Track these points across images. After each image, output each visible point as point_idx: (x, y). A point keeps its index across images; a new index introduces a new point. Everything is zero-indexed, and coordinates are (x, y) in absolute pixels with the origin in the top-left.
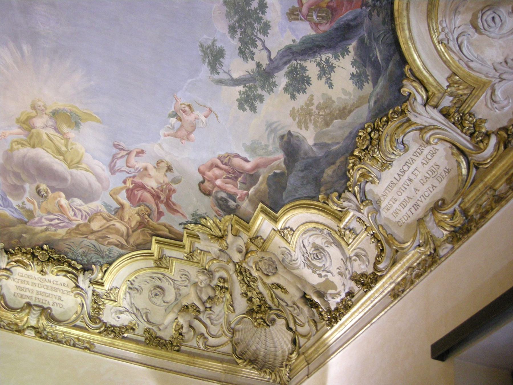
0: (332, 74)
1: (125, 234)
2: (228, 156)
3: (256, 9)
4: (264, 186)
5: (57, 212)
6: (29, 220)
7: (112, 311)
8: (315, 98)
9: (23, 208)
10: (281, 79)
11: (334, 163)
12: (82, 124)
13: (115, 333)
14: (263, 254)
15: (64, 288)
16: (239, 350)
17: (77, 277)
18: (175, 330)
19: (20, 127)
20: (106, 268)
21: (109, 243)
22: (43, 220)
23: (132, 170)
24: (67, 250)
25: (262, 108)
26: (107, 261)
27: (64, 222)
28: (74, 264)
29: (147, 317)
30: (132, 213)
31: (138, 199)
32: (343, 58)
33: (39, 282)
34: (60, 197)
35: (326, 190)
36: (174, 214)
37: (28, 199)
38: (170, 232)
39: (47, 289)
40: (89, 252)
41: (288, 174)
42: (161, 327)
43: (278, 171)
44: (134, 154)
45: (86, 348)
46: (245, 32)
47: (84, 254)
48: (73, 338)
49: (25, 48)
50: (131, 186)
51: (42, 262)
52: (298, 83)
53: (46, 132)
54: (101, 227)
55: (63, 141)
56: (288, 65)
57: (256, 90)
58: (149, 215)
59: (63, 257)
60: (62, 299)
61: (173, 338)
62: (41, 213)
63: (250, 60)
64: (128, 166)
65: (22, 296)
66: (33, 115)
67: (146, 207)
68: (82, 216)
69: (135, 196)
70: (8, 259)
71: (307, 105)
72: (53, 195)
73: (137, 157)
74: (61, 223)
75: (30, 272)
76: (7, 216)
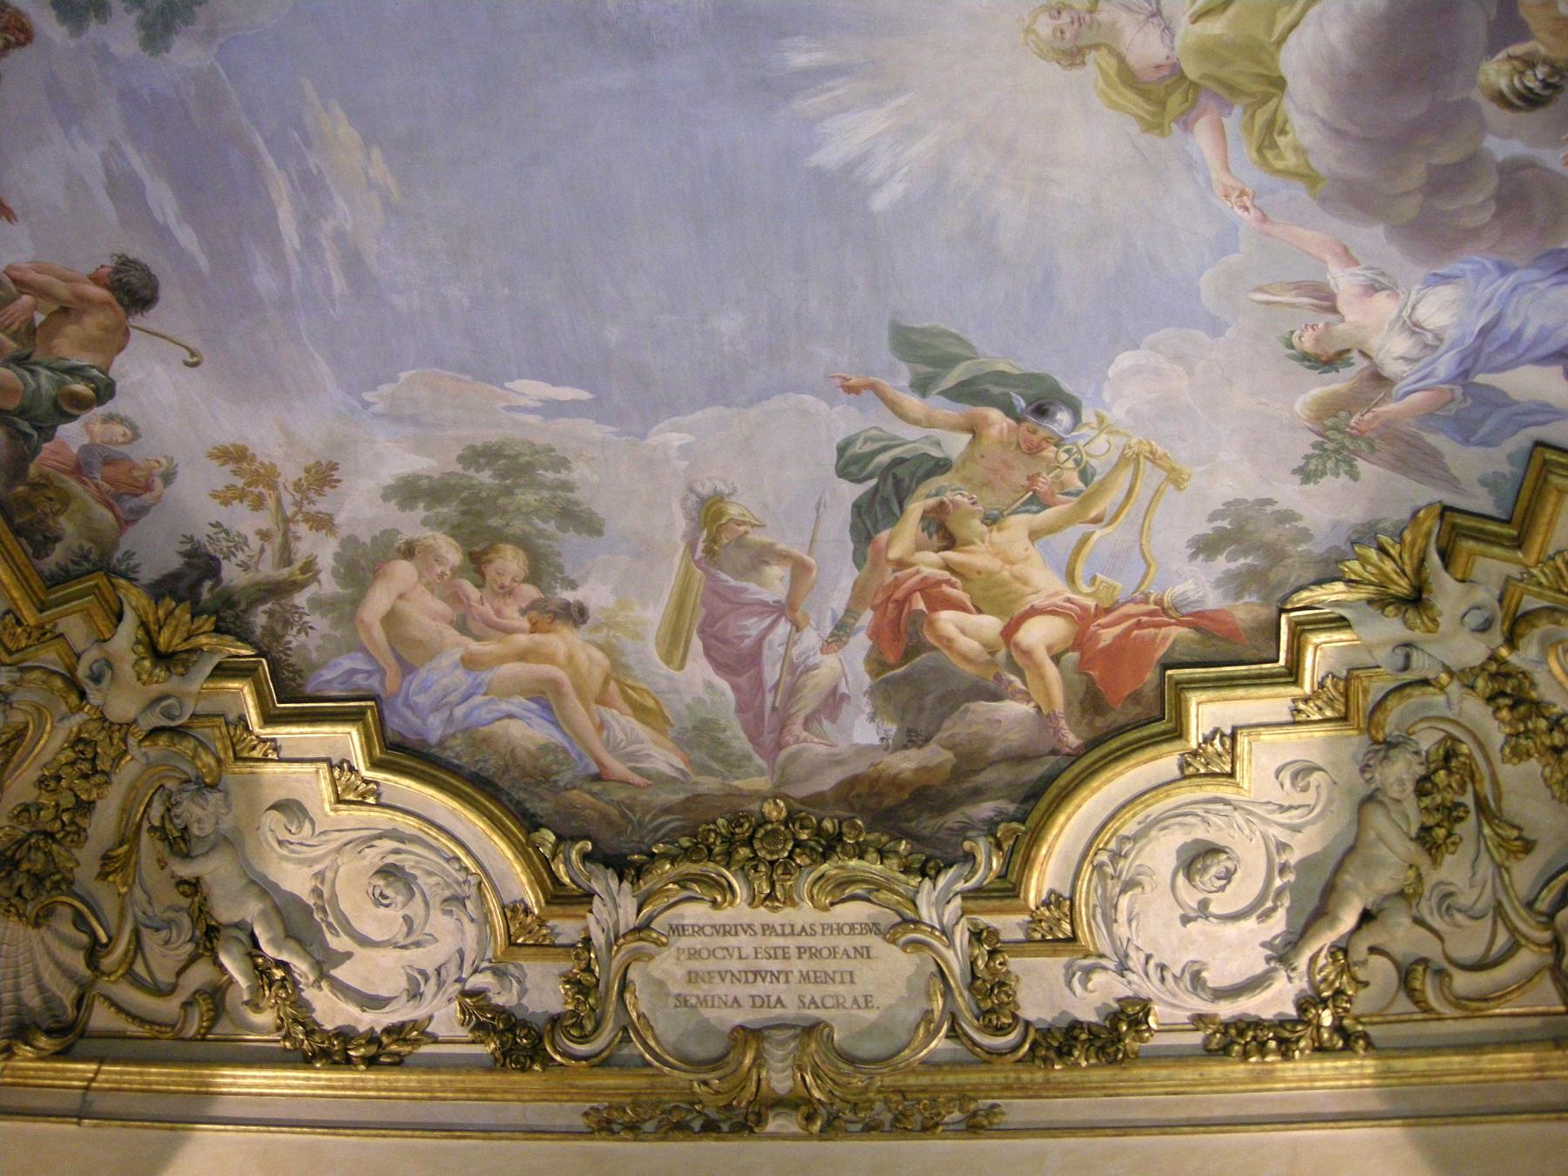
19: (1187, 127)
53: (1185, 19)
66: (1114, 62)
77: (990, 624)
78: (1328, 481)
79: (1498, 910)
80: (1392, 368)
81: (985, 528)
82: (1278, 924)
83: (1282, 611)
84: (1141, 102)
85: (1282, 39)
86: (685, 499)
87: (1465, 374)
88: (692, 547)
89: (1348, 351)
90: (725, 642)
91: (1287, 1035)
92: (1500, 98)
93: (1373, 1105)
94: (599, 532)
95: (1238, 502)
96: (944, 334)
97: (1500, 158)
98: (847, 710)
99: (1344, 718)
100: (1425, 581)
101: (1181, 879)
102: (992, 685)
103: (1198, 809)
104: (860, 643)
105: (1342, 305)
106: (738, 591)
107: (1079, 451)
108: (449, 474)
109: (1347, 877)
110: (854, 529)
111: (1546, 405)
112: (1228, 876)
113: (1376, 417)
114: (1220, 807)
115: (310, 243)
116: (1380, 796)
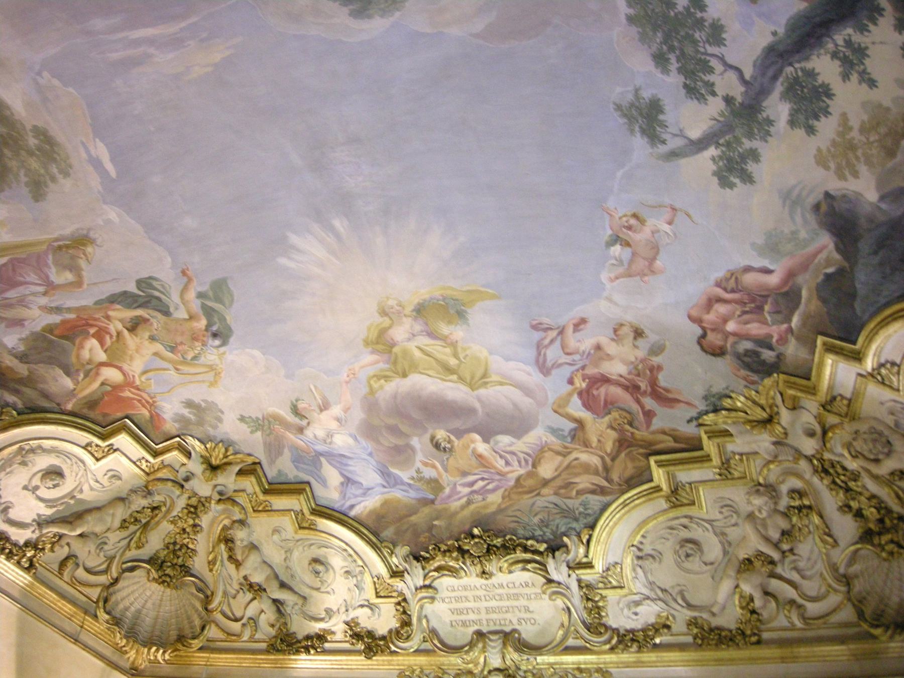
0: (867, 61)
1: (600, 468)
2: (732, 274)
3: (687, 9)
5: (477, 468)
6: (436, 495)
7: (621, 605)
8: (850, 116)
9: (421, 479)
10: (778, 108)
12: (469, 311)
13: (638, 642)
14: (856, 426)
15: (527, 591)
16: (868, 611)
17: (545, 566)
18: (742, 608)
19: (372, 353)
20: (587, 537)
21: (579, 493)
22: (459, 488)
23: (577, 357)
24: (513, 525)
25: (760, 170)
27: (492, 481)
28: (532, 546)
29: (684, 599)
30: (599, 428)
31: (602, 403)
32: (876, 24)
33: (485, 592)
34: (473, 441)
36: (672, 407)
37: (423, 462)
38: (676, 439)
39: (501, 600)
40: (551, 518)
41: (852, 268)
42: (715, 610)
43: (830, 270)
44: (570, 330)
46: (683, 53)
47: (544, 524)
50: (584, 385)
51: (479, 557)
52: (810, 102)
53: (416, 344)
54: (556, 470)
55: (448, 350)
56: (781, 79)
57: (740, 143)
58: (631, 424)
59: (510, 539)
60: (531, 609)
61: (741, 623)
62: (451, 478)
63: (710, 98)
64: (568, 354)
65: (464, 624)
66: (388, 325)
67: (621, 412)
68: (519, 462)
69: (596, 398)
70: (423, 568)
71: (841, 134)
74: (488, 484)
75: (465, 581)
76: (399, 501)
77: (102, 357)
78: (244, 426)
79: (111, 559)
81: (147, 337)
82: (49, 512)
83: (179, 436)
84: (376, 335)
85: (421, 373)
86: (82, 229)
87: (322, 455)
88: (57, 240)
90: (14, 270)
91: (14, 551)
92: (432, 438)
93: (16, 594)
94: (37, 201)
95: (216, 405)
96: (232, 295)
98: (18, 329)
99: (148, 474)
100: (225, 470)
101: (40, 475)
102: (73, 370)
103: (74, 459)
104: (56, 319)
105: (325, 413)
106: (47, 265)
108: (22, 124)
109: (90, 518)
110: (113, 295)
112: (55, 486)
114: (81, 465)
115: (137, 43)
116: (127, 502)
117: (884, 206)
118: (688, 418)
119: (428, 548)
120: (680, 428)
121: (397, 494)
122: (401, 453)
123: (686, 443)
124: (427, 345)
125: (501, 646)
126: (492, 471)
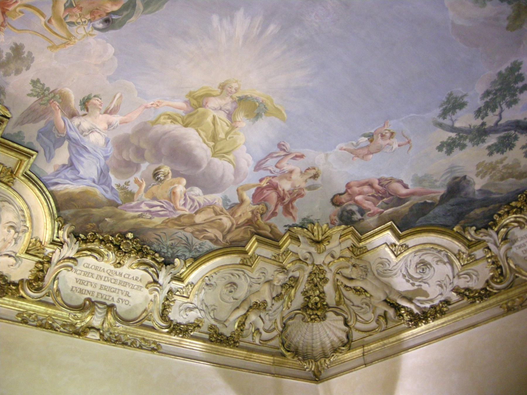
3: (518, 88)
4: (407, 209)
5: (165, 199)
6: (124, 203)
7: (181, 308)
10: (492, 140)
11: (486, 206)
12: (264, 117)
14: (357, 262)
15: (135, 283)
19: (186, 102)
21: (204, 238)
23: (278, 170)
26: (193, 256)
27: (167, 209)
35: (465, 223)
36: (286, 216)
39: (114, 283)
40: (178, 245)
42: (226, 324)
43: (428, 201)
45: (153, 350)
46: (495, 99)
47: (172, 247)
48: (138, 339)
49: (272, 28)
50: (265, 185)
53: (215, 114)
55: (227, 128)
56: (506, 132)
57: (465, 139)
58: (262, 215)
60: (130, 295)
62: (144, 197)
63: (480, 118)
65: (81, 291)
66: (215, 94)
68: (191, 206)
69: (262, 194)
71: (497, 162)
72: (172, 180)
73: (292, 160)
75: (102, 264)
76: (95, 195)
80: (76, 121)
85: (197, 131)
87: (69, 139)
89: (88, 111)
92: (159, 168)
96: (157, 9)
97: (142, 165)
107: (83, 25)
111: (53, 157)
113: (56, 109)
117: (477, 193)
118: (286, 224)
119: (87, 233)
120: (278, 228)
121: (99, 191)
122: (128, 167)
123: (274, 236)
124: (220, 119)
125: (105, 313)
126: (172, 204)
